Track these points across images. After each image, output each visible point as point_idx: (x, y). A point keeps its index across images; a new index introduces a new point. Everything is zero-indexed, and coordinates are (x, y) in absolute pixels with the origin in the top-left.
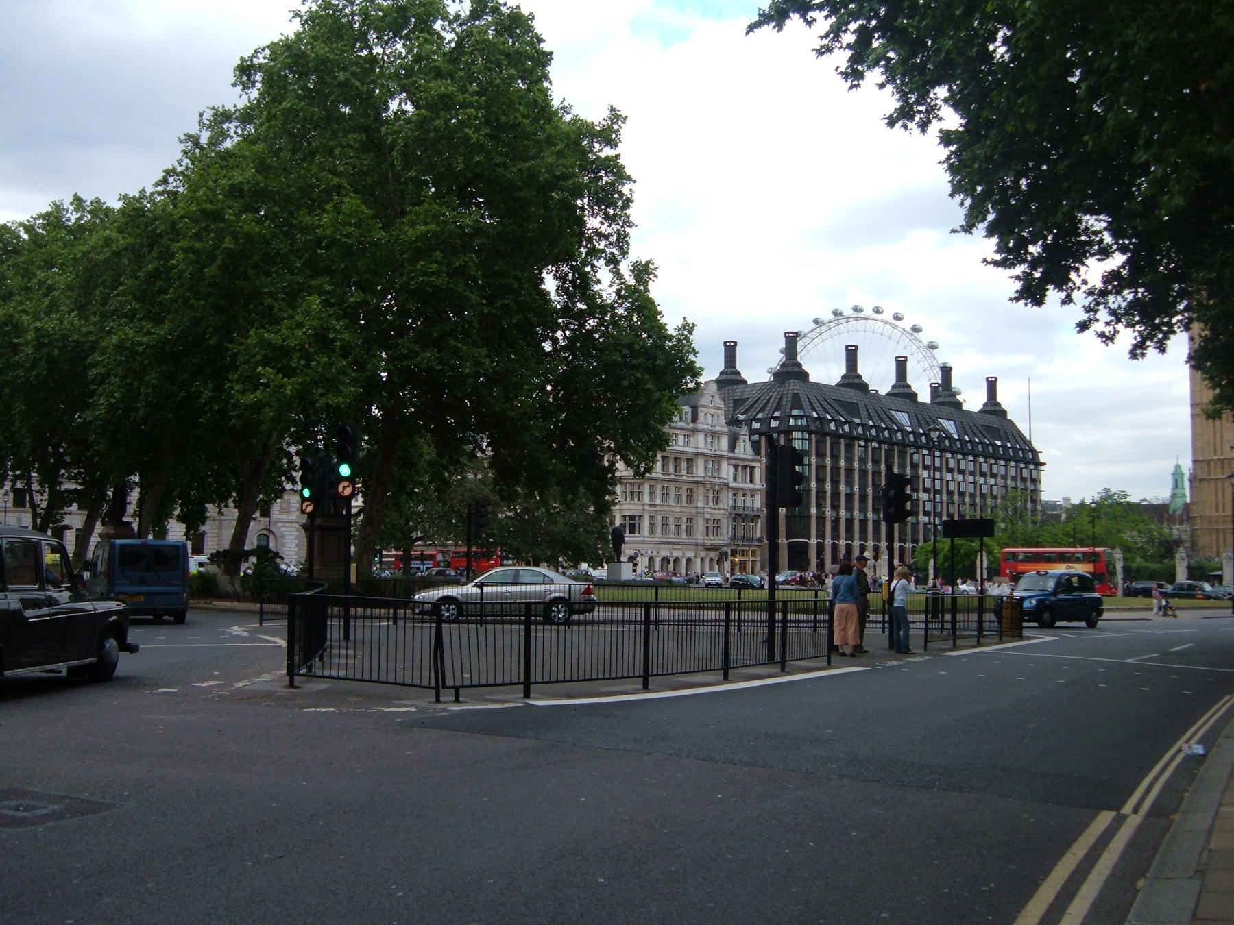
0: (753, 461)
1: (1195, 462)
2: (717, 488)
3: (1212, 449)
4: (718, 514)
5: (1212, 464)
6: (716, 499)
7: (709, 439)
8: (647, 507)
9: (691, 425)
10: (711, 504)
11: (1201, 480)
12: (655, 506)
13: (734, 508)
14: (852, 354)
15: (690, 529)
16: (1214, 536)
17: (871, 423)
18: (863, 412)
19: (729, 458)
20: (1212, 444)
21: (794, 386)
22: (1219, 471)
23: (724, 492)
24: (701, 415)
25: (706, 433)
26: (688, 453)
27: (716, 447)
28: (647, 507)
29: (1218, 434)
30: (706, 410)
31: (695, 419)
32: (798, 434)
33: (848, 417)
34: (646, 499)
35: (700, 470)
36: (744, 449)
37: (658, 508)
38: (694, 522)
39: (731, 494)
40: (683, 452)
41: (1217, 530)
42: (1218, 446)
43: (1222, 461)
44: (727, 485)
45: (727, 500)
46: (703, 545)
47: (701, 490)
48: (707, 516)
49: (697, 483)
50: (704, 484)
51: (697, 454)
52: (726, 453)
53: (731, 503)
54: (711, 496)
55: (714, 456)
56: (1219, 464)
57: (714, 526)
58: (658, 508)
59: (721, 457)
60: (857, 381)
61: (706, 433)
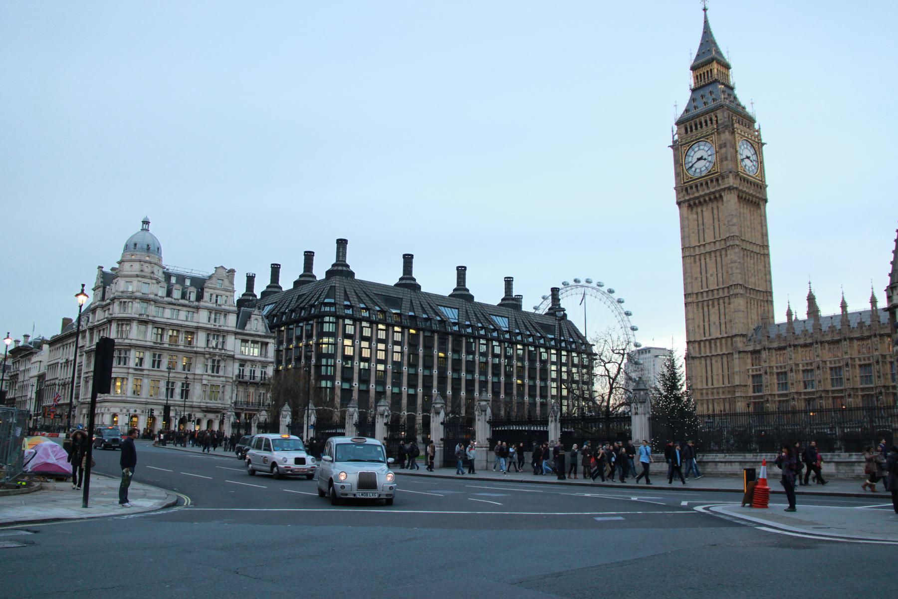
0: (265, 337)
1: (688, 343)
2: (217, 358)
3: (702, 331)
4: (219, 381)
5: (702, 344)
6: (216, 368)
7: (213, 316)
8: (131, 371)
9: (197, 303)
10: (210, 372)
11: (693, 358)
12: (142, 370)
13: (240, 375)
14: (408, 260)
15: (185, 393)
16: (705, 406)
17: (480, 325)
18: (406, 304)
19: (236, 333)
20: (702, 327)
21: (336, 281)
22: (708, 350)
23: (230, 362)
24: (206, 296)
25: (210, 310)
26: (187, 326)
27: (222, 323)
28: (131, 371)
29: (706, 319)
30: (212, 291)
31: (200, 297)
32: (327, 319)
33: (385, 308)
34: (132, 363)
35: (200, 341)
36: (257, 325)
37: (145, 372)
38: (191, 387)
39: (237, 365)
40: (181, 326)
41: (707, 400)
42: (707, 329)
43: (710, 341)
44: (233, 357)
45: (233, 370)
46: (199, 407)
47: (201, 359)
48: (205, 382)
49: (196, 353)
50: (203, 354)
51: (198, 328)
52: (234, 329)
53: (237, 372)
54: (210, 364)
55: (219, 331)
56: (707, 343)
57: (214, 390)
58: (145, 372)
59: (228, 332)
60: (466, 293)
61: (210, 310)
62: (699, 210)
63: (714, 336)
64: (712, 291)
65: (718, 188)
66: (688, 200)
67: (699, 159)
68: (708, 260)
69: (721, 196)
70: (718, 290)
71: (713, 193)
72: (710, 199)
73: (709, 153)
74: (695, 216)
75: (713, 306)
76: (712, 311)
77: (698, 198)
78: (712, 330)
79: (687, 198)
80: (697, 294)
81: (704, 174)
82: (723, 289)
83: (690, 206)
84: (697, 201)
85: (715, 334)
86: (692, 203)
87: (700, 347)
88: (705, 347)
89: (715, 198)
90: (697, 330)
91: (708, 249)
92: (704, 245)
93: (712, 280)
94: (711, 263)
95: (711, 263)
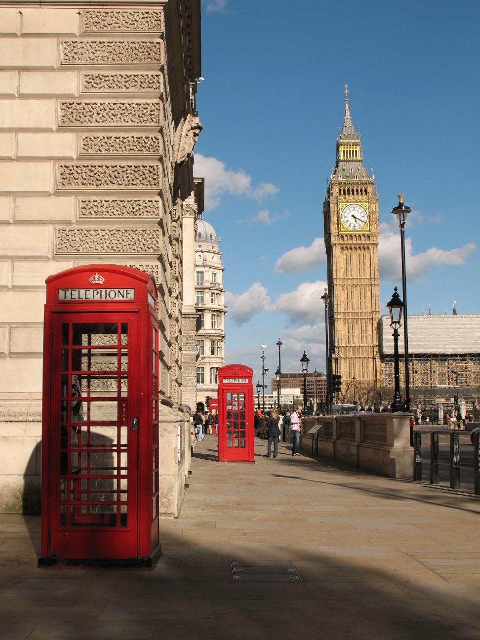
62: (349, 252)
63: (357, 344)
64: (357, 313)
65: (368, 242)
66: (342, 244)
67: (353, 216)
68: (354, 290)
69: (368, 248)
70: (361, 313)
71: (363, 244)
72: (359, 248)
73: (362, 215)
74: (345, 257)
75: (357, 324)
76: (356, 326)
77: (351, 244)
78: (356, 340)
79: (342, 242)
80: (343, 313)
81: (357, 229)
82: (365, 312)
83: (342, 248)
84: (349, 247)
85: (357, 342)
86: (344, 246)
87: (345, 351)
88: (349, 351)
89: (364, 248)
90: (343, 338)
91: (355, 282)
92: (351, 279)
93: (356, 305)
94: (356, 292)
95: (356, 292)
